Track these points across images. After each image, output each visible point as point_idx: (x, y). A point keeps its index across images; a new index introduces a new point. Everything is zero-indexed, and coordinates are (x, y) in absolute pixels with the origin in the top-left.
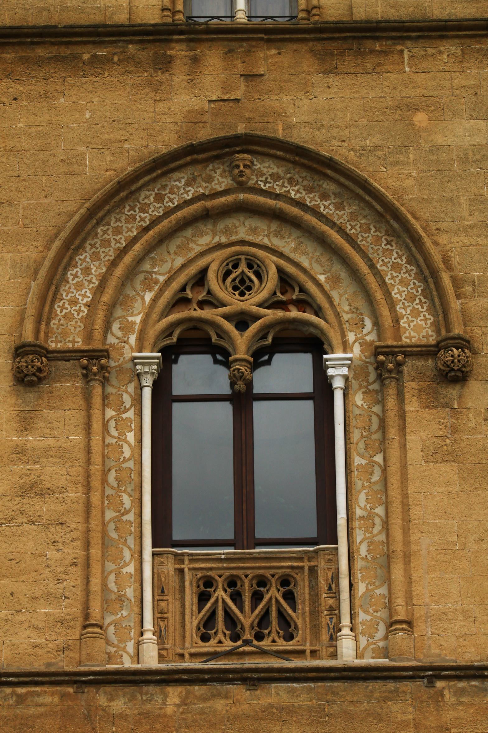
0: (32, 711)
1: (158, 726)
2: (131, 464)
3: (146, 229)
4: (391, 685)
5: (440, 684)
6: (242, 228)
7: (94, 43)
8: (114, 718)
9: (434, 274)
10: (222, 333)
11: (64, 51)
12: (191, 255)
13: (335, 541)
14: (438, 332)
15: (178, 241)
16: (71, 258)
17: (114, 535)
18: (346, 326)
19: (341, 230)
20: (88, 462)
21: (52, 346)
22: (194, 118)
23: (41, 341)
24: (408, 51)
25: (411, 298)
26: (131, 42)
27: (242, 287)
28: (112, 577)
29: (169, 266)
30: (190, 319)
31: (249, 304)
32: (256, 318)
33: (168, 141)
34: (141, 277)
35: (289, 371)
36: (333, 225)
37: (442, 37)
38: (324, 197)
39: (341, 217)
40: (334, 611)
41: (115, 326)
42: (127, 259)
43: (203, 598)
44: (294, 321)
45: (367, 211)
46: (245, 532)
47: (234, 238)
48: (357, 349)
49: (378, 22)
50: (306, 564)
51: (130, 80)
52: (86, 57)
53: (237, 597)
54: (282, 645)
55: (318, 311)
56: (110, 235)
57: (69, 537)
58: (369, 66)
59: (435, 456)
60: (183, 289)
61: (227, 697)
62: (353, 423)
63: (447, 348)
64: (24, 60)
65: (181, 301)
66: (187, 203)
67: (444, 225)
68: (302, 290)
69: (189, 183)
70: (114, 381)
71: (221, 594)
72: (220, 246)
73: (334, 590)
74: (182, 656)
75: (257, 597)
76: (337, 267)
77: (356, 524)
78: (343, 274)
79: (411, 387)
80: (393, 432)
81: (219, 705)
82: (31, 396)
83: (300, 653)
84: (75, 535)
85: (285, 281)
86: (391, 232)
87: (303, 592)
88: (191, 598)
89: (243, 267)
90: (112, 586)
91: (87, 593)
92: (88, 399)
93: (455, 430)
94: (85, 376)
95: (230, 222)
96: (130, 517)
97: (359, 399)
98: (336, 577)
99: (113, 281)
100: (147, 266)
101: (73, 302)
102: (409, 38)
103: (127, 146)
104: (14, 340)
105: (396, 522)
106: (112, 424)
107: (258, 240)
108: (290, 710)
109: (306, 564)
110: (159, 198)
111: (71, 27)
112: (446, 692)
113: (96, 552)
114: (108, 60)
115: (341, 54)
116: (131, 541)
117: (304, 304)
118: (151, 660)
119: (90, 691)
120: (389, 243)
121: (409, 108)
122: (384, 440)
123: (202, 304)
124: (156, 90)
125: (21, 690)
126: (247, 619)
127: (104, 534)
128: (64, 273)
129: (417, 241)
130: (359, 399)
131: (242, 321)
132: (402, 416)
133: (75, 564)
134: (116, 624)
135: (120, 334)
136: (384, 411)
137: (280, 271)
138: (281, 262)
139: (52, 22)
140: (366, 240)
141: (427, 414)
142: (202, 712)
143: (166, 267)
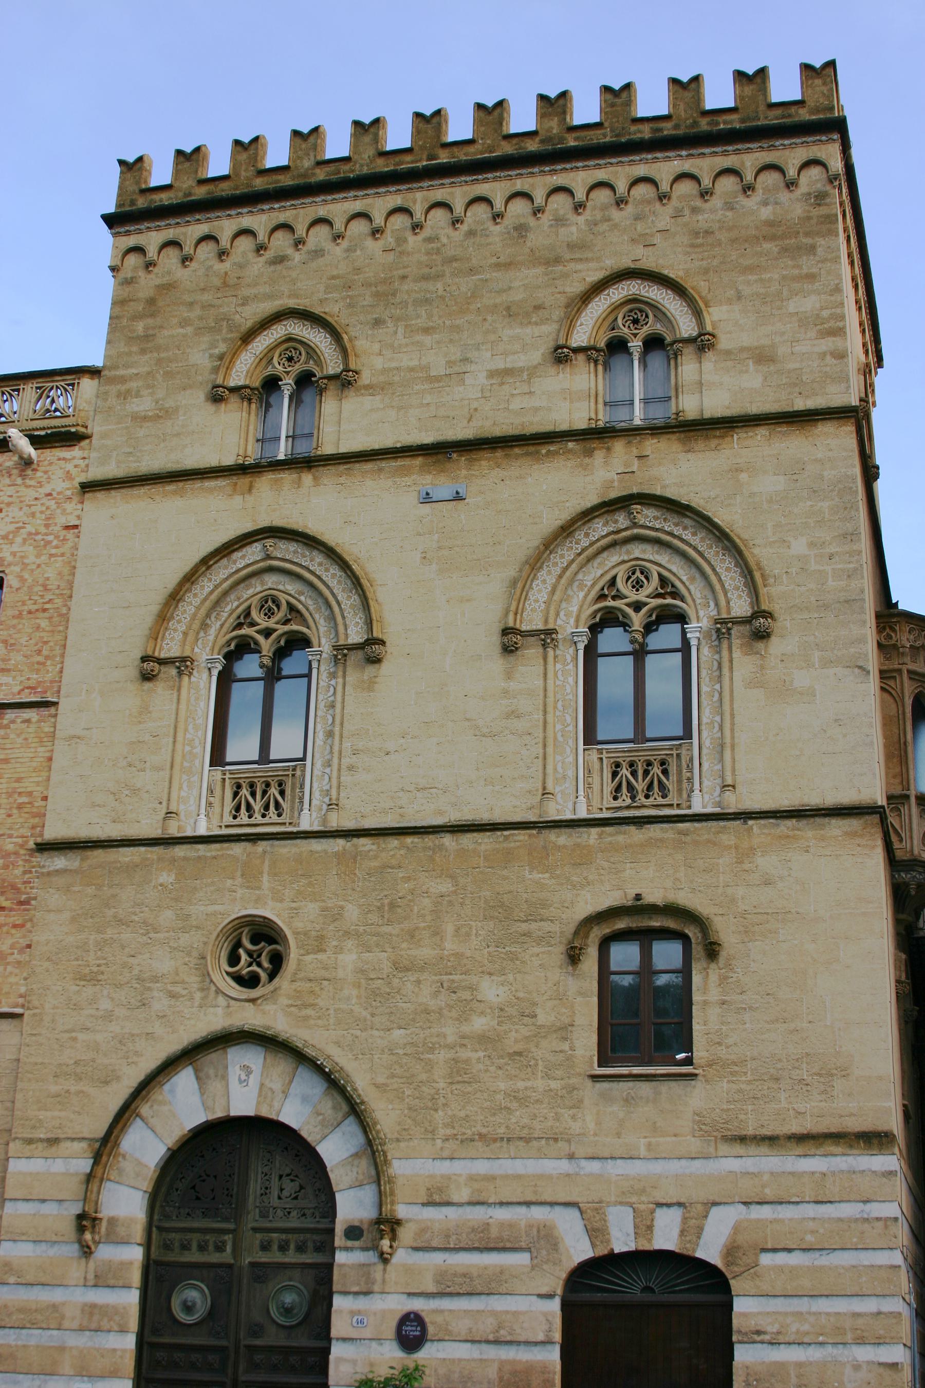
0: (512, 845)
1: (585, 851)
2: (570, 697)
3: (579, 554)
4: (722, 823)
5: (750, 822)
6: (638, 550)
8: (559, 848)
9: (750, 573)
10: (625, 615)
12: (606, 568)
14: (753, 608)
15: (598, 560)
16: (535, 575)
17: (560, 739)
18: (699, 607)
19: (695, 549)
20: (545, 696)
21: (524, 628)
22: (608, 485)
23: (518, 626)
25: (737, 588)
26: (570, 441)
27: (638, 585)
28: (560, 765)
29: (594, 575)
30: (606, 607)
31: (641, 596)
32: (646, 604)
33: (592, 500)
34: (577, 583)
35: (668, 635)
36: (690, 545)
37: (757, 425)
38: (685, 528)
39: (695, 540)
40: (690, 780)
41: (562, 614)
42: (568, 573)
43: (615, 774)
44: (668, 605)
45: (711, 536)
46: (640, 735)
47: (632, 557)
48: (705, 620)
49: (718, 418)
50: (674, 752)
51: (569, 464)
52: (544, 451)
53: (634, 774)
54: (660, 801)
55: (683, 599)
56: (558, 560)
57: (534, 741)
58: (713, 446)
59: (751, 684)
60: (603, 589)
61: (625, 833)
62: (702, 666)
63: (757, 618)
65: (602, 597)
66: (604, 537)
67: (757, 542)
68: (673, 586)
69: (604, 525)
70: (561, 647)
71: (625, 772)
72: (624, 562)
73: (690, 769)
74: (601, 809)
75: (646, 773)
76: (694, 570)
77: (703, 727)
78: (697, 575)
79: (736, 642)
80: (726, 671)
81: (620, 838)
82: (512, 658)
83: (671, 805)
84: (537, 740)
85: (663, 581)
86: (725, 548)
87: (673, 769)
88: (607, 775)
89: (638, 574)
90: (560, 770)
91: (545, 774)
92: (545, 659)
93: (762, 667)
94: (543, 645)
95: (629, 547)
96: (571, 728)
97: (705, 651)
98: (691, 760)
99: (560, 587)
100: (580, 576)
101: (537, 601)
102: (737, 427)
103: (568, 504)
104: (502, 626)
105: (727, 725)
106: (560, 673)
107: (646, 557)
108: (662, 840)
109: (674, 752)
110: (587, 535)
112: (755, 827)
113: (550, 750)
114: (556, 453)
115: (696, 440)
116: (571, 742)
117: (675, 594)
118: (582, 814)
119: (546, 832)
120: (724, 555)
121: (737, 470)
122: (720, 676)
123: (614, 598)
124: (585, 469)
125: (506, 833)
126: (640, 786)
127: (555, 739)
128: (531, 584)
129: (740, 553)
130: (705, 651)
131: (637, 606)
132: (731, 661)
133: (537, 758)
134: (562, 792)
135: (564, 618)
136: (721, 658)
137: (660, 575)
138: (660, 570)
140: (710, 554)
141: (747, 659)
142: (610, 843)
143: (592, 576)
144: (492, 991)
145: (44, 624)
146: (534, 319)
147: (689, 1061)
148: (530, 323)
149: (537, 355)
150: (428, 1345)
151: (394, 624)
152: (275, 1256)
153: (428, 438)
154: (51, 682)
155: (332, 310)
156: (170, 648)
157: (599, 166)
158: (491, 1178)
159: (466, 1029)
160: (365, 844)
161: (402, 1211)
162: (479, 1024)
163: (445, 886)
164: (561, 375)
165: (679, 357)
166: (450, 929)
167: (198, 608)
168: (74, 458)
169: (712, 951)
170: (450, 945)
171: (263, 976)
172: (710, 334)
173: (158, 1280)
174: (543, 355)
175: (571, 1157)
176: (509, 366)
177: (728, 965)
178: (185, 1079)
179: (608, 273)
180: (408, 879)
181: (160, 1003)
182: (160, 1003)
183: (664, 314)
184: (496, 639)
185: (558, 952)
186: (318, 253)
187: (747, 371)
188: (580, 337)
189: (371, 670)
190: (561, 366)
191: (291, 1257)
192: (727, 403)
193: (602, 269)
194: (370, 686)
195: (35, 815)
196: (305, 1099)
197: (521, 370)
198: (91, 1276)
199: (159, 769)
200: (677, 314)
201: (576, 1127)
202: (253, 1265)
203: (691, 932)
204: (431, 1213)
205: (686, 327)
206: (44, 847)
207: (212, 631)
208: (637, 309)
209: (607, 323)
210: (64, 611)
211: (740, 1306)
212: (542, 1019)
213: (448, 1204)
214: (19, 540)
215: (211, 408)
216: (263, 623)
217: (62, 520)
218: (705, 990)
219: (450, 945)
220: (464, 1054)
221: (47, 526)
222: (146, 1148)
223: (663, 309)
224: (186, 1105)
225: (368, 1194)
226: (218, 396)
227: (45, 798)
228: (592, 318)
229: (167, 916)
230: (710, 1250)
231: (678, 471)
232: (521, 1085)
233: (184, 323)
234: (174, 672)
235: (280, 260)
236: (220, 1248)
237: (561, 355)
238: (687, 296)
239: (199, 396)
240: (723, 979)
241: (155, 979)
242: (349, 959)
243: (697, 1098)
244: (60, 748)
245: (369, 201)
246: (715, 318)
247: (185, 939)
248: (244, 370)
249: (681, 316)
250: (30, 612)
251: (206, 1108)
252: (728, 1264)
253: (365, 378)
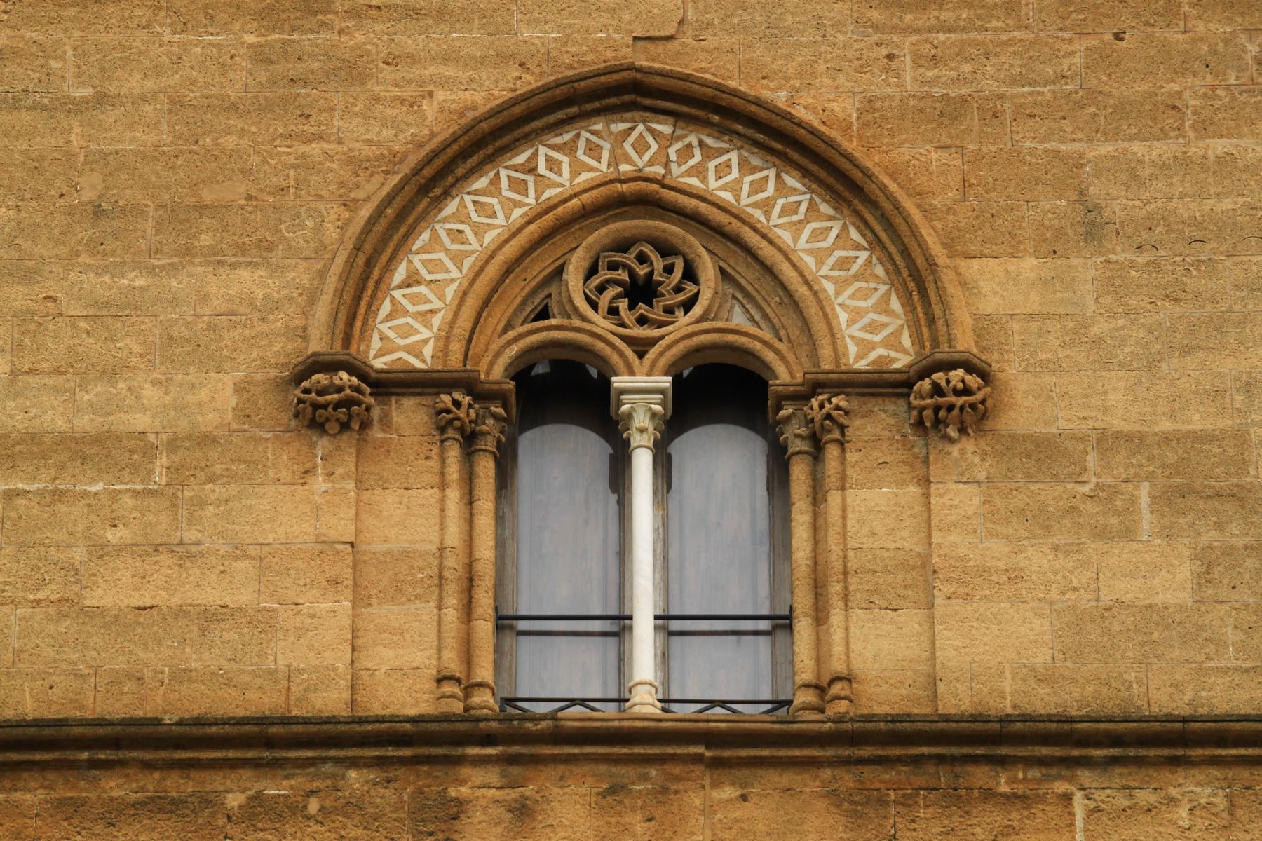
7: (256, 764)
11: (178, 785)
26: (354, 763)
37: (1175, 762)
49: (1006, 719)
52: (234, 800)
64: (70, 809)
102: (1086, 762)
111: (198, 722)
114: (293, 810)
115: (907, 802)
139: (147, 710)
146: (205, 240)
148: (187, 252)
164: (320, 483)
165: (832, 452)
172: (970, 368)
174: (240, 389)
176: (85, 423)
179: (530, 82)
183: (768, 270)
187: (1128, 533)
188: (408, 331)
190: (323, 445)
192: (1041, 658)
193: (504, 59)
197: (141, 448)
200: (825, 275)
205: (864, 325)
208: (644, 247)
209: (517, 290)
223: (766, 251)
228: (457, 259)
238: (874, 205)
246: (990, 304)
249: (841, 284)
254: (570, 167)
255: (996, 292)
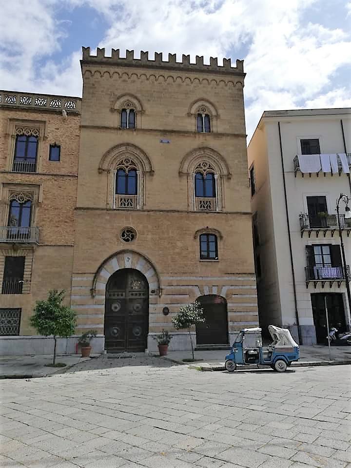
13: (215, 197)
24: (224, 138)
29: (196, 163)
33: (196, 146)
39: (217, 158)
65: (197, 168)
71: (202, 203)
87: (212, 203)
141: (227, 183)
144: (179, 244)
145: (72, 157)
147: (217, 259)
149: (184, 114)
150: (169, 314)
151: (156, 167)
152: (134, 297)
153: (161, 129)
154: (76, 171)
155: (139, 95)
156: (105, 167)
157: (197, 74)
158: (180, 280)
159: (175, 251)
160: (151, 213)
161: (162, 287)
162: (177, 250)
163: (169, 223)
166: (170, 231)
167: (111, 159)
168: (76, 119)
169: (221, 237)
170: (171, 235)
171: (130, 239)
173: (108, 303)
175: (196, 277)
177: (225, 241)
178: (114, 261)
180: (161, 221)
181: (108, 244)
182: (108, 244)
184: (178, 174)
185: (192, 238)
186: (134, 82)
189: (151, 177)
191: (138, 297)
194: (152, 180)
195: (74, 201)
196: (141, 265)
198: (94, 302)
199: (105, 194)
201: (197, 271)
202: (129, 299)
203: (217, 235)
204: (168, 287)
206: (76, 209)
207: (114, 164)
210: (78, 155)
211: (229, 305)
212: (190, 249)
213: (172, 286)
214: (64, 137)
215: (110, 113)
216: (126, 165)
217: (75, 134)
218: (220, 246)
219: (171, 235)
220: (174, 256)
221: (71, 135)
222: (106, 275)
224: (115, 266)
225: (156, 284)
226: (112, 110)
227: (76, 198)
229: (108, 226)
230: (223, 295)
231: (212, 143)
232: (186, 262)
233: (102, 92)
234: (106, 173)
235: (124, 81)
236: (122, 295)
237: (189, 115)
239: (108, 110)
240: (224, 244)
241: (106, 239)
242: (150, 237)
243: (219, 266)
244: (79, 186)
245: (146, 71)
247: (113, 231)
248: (117, 106)
250: (68, 154)
251: (119, 266)
252: (227, 297)
253: (147, 112)
254: (200, 103)
255: (220, 111)
